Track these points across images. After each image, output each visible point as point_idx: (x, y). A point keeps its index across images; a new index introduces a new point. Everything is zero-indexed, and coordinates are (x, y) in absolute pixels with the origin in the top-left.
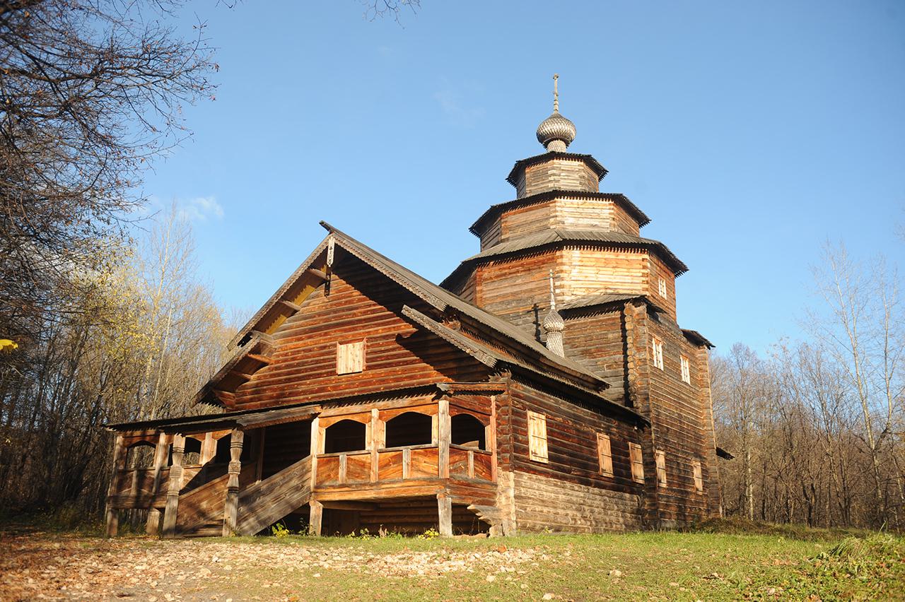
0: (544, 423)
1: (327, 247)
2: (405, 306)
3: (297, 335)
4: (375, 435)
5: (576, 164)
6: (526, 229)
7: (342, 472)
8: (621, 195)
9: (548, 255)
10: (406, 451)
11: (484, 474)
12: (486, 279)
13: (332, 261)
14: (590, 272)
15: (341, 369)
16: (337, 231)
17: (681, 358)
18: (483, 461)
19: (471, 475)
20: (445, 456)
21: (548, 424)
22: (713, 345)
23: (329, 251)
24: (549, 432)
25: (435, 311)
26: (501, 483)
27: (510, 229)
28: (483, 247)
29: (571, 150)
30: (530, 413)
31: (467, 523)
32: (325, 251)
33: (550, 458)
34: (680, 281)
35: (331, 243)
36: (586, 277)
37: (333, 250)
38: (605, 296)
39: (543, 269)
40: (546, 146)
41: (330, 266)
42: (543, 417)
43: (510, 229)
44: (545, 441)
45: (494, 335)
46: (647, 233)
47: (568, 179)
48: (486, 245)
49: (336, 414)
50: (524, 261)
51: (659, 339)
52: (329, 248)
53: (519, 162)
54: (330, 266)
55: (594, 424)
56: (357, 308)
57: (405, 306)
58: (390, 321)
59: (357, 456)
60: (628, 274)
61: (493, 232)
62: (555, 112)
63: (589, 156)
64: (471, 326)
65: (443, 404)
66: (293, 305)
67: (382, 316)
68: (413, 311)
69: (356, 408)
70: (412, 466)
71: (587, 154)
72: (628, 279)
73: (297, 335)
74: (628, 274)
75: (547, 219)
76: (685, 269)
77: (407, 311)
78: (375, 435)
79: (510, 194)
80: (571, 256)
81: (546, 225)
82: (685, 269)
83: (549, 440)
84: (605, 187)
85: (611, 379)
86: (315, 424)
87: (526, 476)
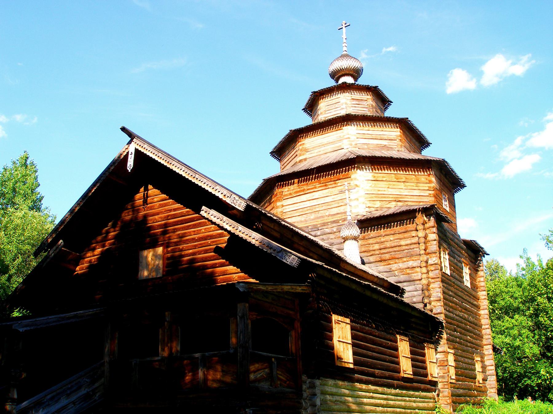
0: (349, 327)
1: (128, 153)
2: (204, 208)
8: (408, 118)
11: (288, 382)
12: (286, 195)
13: (132, 165)
16: (139, 137)
17: (463, 265)
21: (352, 329)
22: (488, 253)
23: (130, 156)
24: (353, 337)
25: (234, 211)
27: (306, 150)
29: (361, 81)
30: (335, 317)
32: (127, 156)
33: (355, 363)
34: (459, 196)
35: (132, 149)
36: (379, 191)
37: (133, 156)
38: (397, 208)
39: (339, 184)
40: (337, 81)
41: (130, 171)
42: (348, 321)
43: (306, 150)
44: (350, 347)
45: (295, 239)
46: (428, 153)
47: (358, 107)
48: (285, 167)
51: (445, 246)
52: (130, 153)
53: (315, 92)
54: (130, 171)
56: (158, 214)
57: (204, 208)
58: (190, 226)
60: (416, 188)
61: (291, 154)
62: (345, 53)
63: (376, 87)
64: (273, 229)
67: (182, 220)
68: (213, 212)
71: (374, 85)
72: (416, 193)
74: (416, 188)
75: (340, 140)
76: (463, 186)
77: (206, 212)
79: (306, 121)
81: (340, 146)
82: (463, 186)
83: (354, 345)
84: (390, 113)
85: (405, 284)
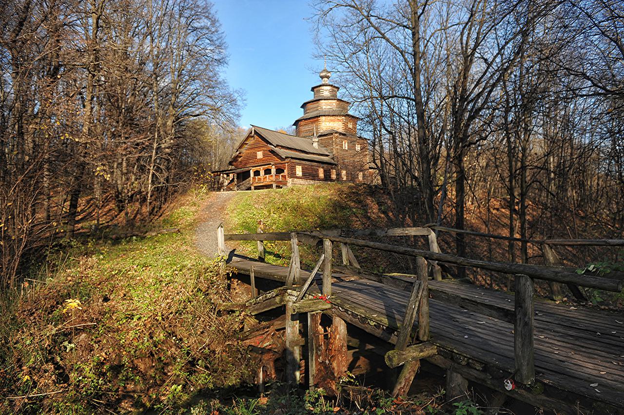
3: (248, 149)
4: (262, 173)
5: (329, 88)
6: (313, 110)
7: (257, 181)
9: (317, 119)
10: (267, 176)
14: (327, 124)
15: (258, 158)
18: (284, 177)
19: (280, 180)
20: (274, 177)
26: (288, 181)
28: (305, 113)
31: (278, 187)
35: (253, 129)
49: (255, 169)
50: (311, 120)
55: (318, 166)
59: (259, 177)
65: (273, 167)
66: (247, 142)
69: (258, 168)
70: (269, 179)
73: (248, 149)
78: (262, 173)
80: (323, 118)
86: (251, 171)
87: (296, 179)
